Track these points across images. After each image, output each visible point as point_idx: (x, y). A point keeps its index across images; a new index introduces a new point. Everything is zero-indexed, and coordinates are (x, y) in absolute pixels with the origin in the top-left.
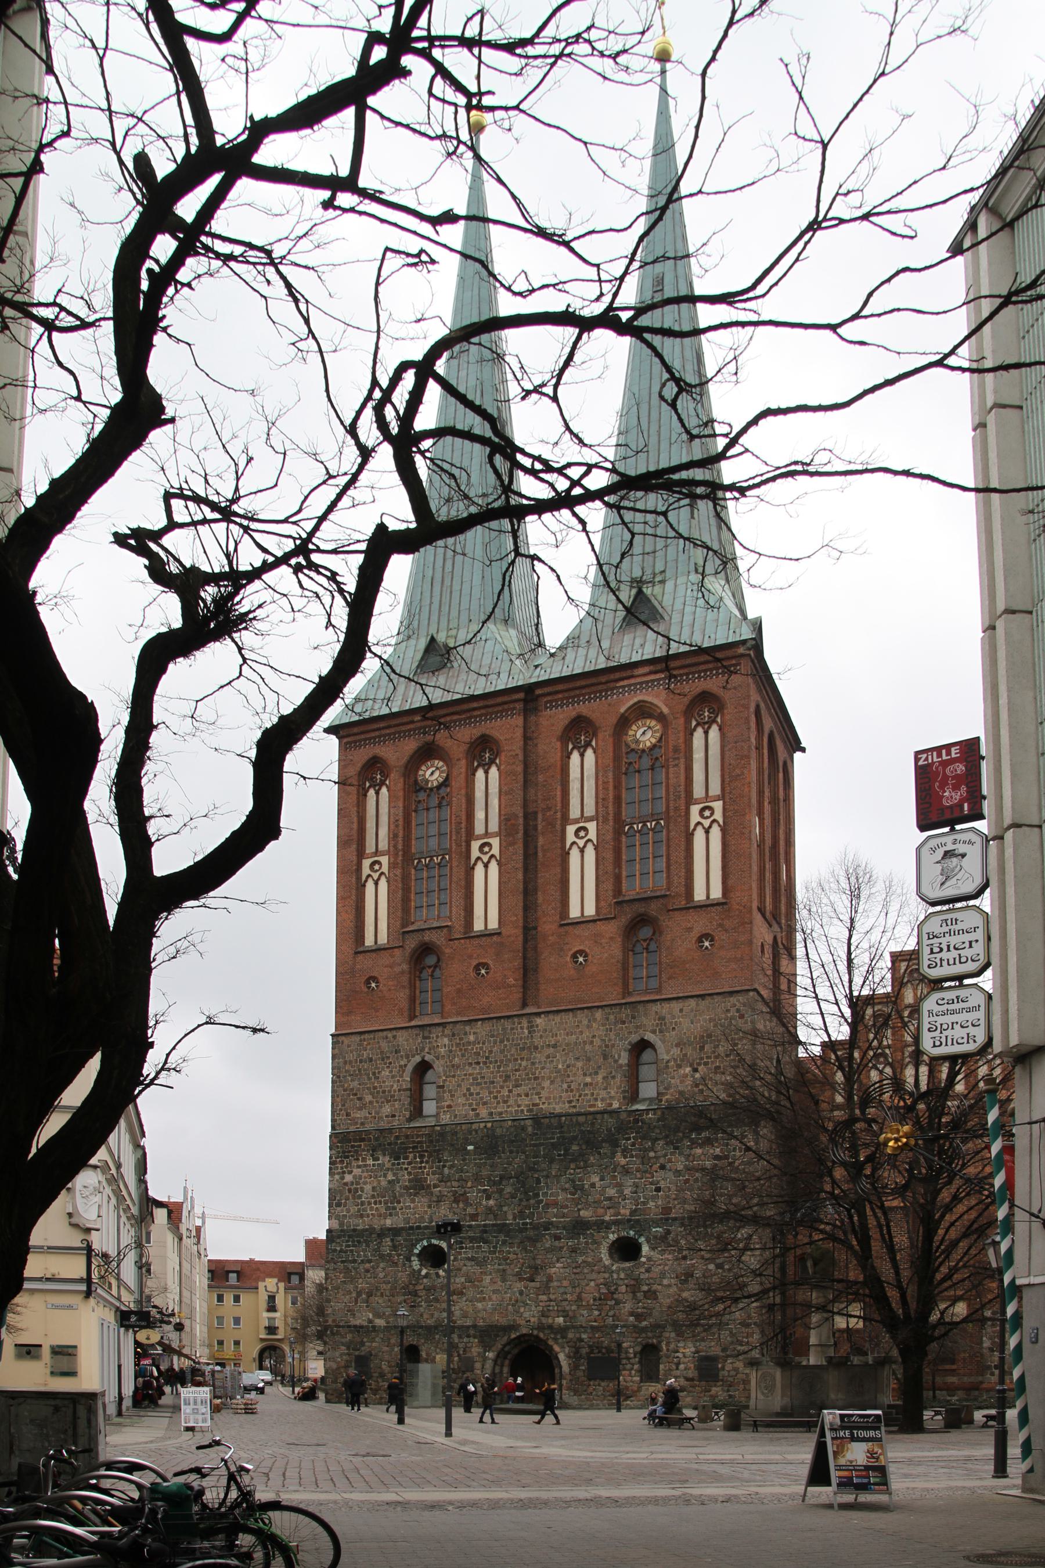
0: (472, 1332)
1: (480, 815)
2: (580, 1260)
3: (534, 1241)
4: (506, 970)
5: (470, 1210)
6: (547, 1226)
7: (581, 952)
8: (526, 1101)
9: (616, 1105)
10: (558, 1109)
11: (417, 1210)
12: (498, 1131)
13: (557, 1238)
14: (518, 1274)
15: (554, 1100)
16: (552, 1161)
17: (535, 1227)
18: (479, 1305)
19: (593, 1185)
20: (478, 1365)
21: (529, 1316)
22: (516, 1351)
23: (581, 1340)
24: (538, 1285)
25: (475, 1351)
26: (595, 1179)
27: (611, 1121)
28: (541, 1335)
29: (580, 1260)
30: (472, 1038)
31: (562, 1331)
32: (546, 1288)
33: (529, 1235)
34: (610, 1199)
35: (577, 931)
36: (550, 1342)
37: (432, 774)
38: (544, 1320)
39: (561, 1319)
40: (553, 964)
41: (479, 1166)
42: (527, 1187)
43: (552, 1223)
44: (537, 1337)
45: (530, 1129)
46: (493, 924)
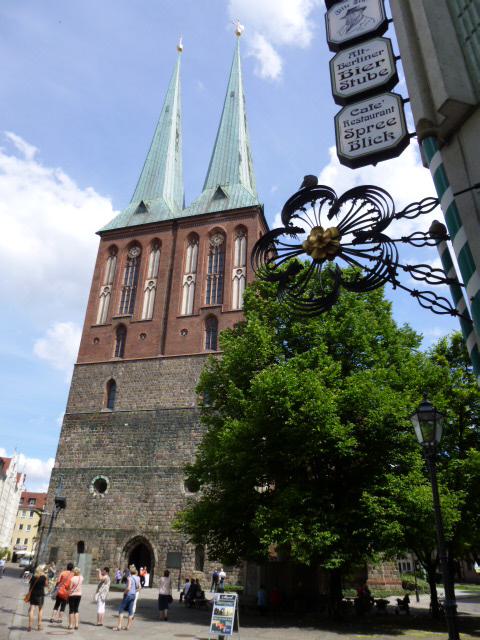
0: (112, 534)
1: (150, 269)
2: (170, 490)
3: (149, 478)
4: (153, 337)
5: (121, 459)
6: (156, 469)
7: (184, 330)
8: (154, 401)
9: (193, 405)
10: (168, 405)
11: (97, 459)
12: (140, 417)
13: (160, 477)
14: (139, 498)
15: (167, 401)
16: (162, 433)
17: (150, 470)
18: (118, 516)
19: (179, 447)
20: (112, 556)
21: (141, 526)
22: (133, 547)
23: (166, 541)
24: (148, 504)
25: (113, 545)
26: (181, 444)
27: (190, 413)
28: (147, 538)
29: (170, 490)
30: (134, 369)
31: (157, 534)
32: (151, 508)
33: (146, 474)
34: (186, 455)
35: (184, 320)
36: (151, 542)
37: (134, 253)
38: (150, 528)
39: (157, 527)
40: (174, 335)
41: (129, 435)
42: (149, 448)
43: (158, 468)
44: (145, 539)
45: (154, 416)
46: (149, 317)
